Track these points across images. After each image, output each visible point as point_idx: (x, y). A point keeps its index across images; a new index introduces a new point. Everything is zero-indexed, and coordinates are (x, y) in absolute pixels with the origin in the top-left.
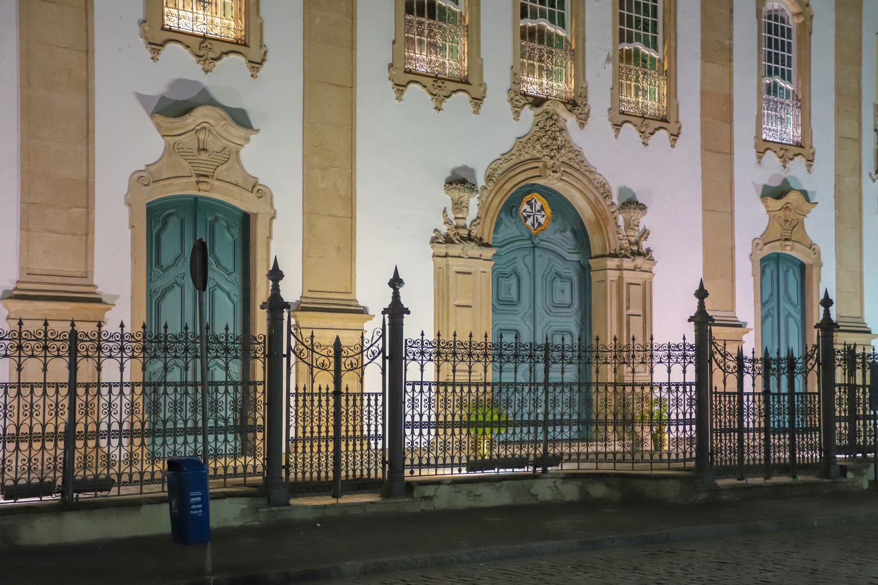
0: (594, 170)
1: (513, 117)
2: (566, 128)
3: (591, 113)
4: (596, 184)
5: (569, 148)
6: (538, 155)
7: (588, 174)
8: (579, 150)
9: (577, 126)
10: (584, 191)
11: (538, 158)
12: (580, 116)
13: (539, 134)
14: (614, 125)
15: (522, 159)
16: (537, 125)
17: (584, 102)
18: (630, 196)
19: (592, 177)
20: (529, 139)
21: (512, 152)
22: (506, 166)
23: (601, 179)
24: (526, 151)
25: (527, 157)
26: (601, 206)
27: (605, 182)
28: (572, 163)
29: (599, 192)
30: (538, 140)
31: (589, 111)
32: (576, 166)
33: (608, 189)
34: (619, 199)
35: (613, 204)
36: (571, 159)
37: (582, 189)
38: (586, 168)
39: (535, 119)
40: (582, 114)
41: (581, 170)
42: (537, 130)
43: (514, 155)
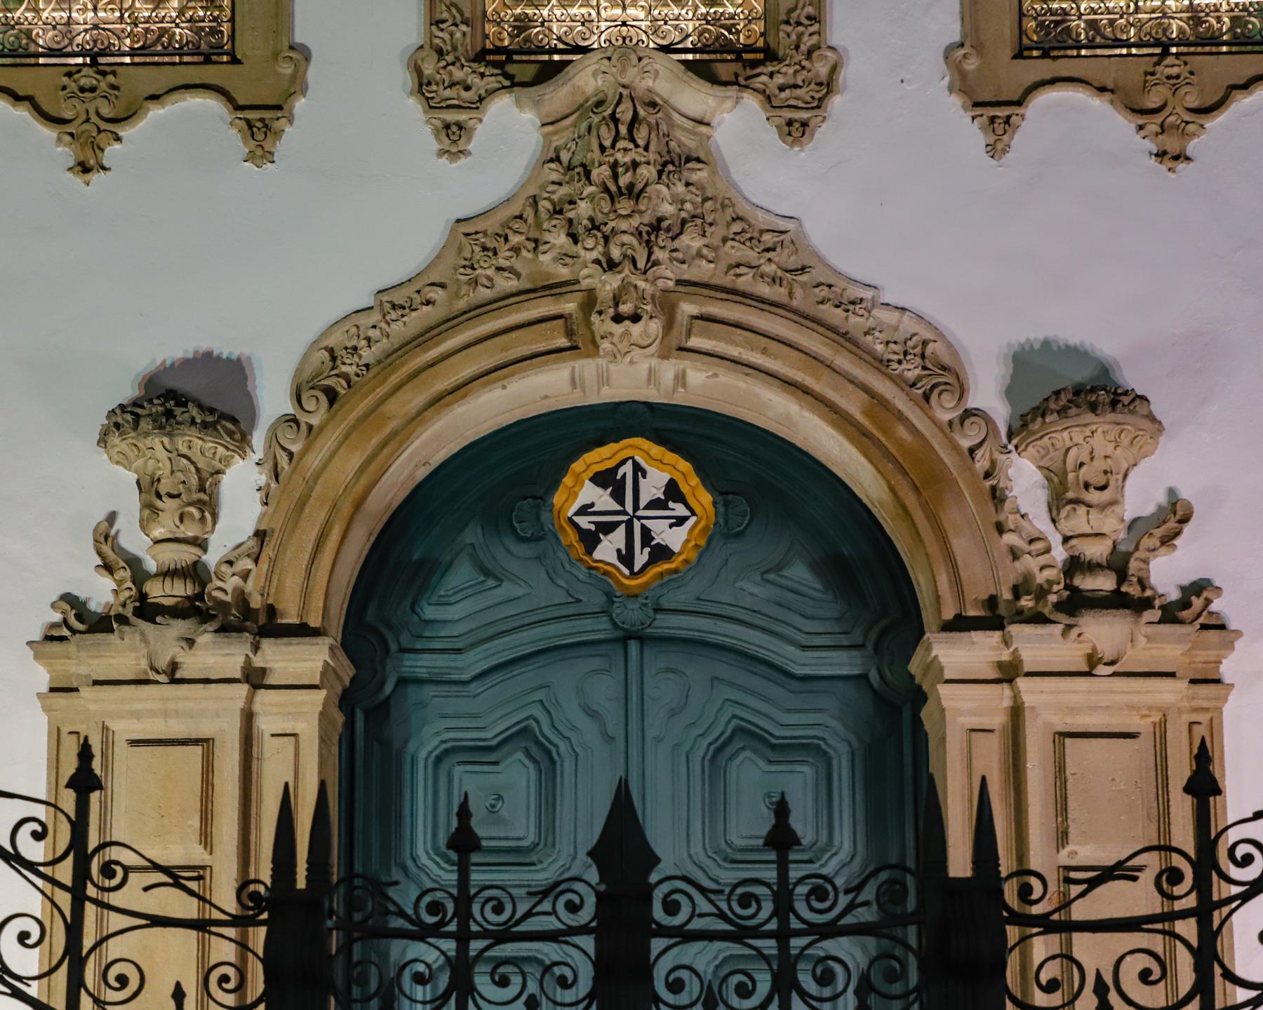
0: (867, 294)
1: (436, 146)
2: (709, 153)
3: (847, 75)
4: (879, 348)
5: (728, 225)
6: (564, 273)
7: (834, 315)
8: (782, 224)
9: (770, 135)
10: (809, 381)
11: (566, 283)
12: (783, 95)
13: (563, 191)
14: (976, 105)
15: (484, 293)
16: (557, 159)
17: (808, 42)
18: (1081, 375)
19: (855, 323)
20: (520, 217)
21: (434, 278)
22: (403, 328)
23: (909, 325)
24: (503, 263)
25: (506, 284)
26: (902, 432)
27: (927, 335)
28: (745, 281)
29: (898, 381)
30: (557, 212)
31: (834, 69)
32: (764, 290)
33: (947, 360)
34: (1011, 393)
35: (968, 413)
36: (738, 265)
37: (798, 376)
38: (823, 292)
39: (545, 136)
40: (796, 86)
41: (795, 303)
42: (555, 177)
43: (442, 286)
